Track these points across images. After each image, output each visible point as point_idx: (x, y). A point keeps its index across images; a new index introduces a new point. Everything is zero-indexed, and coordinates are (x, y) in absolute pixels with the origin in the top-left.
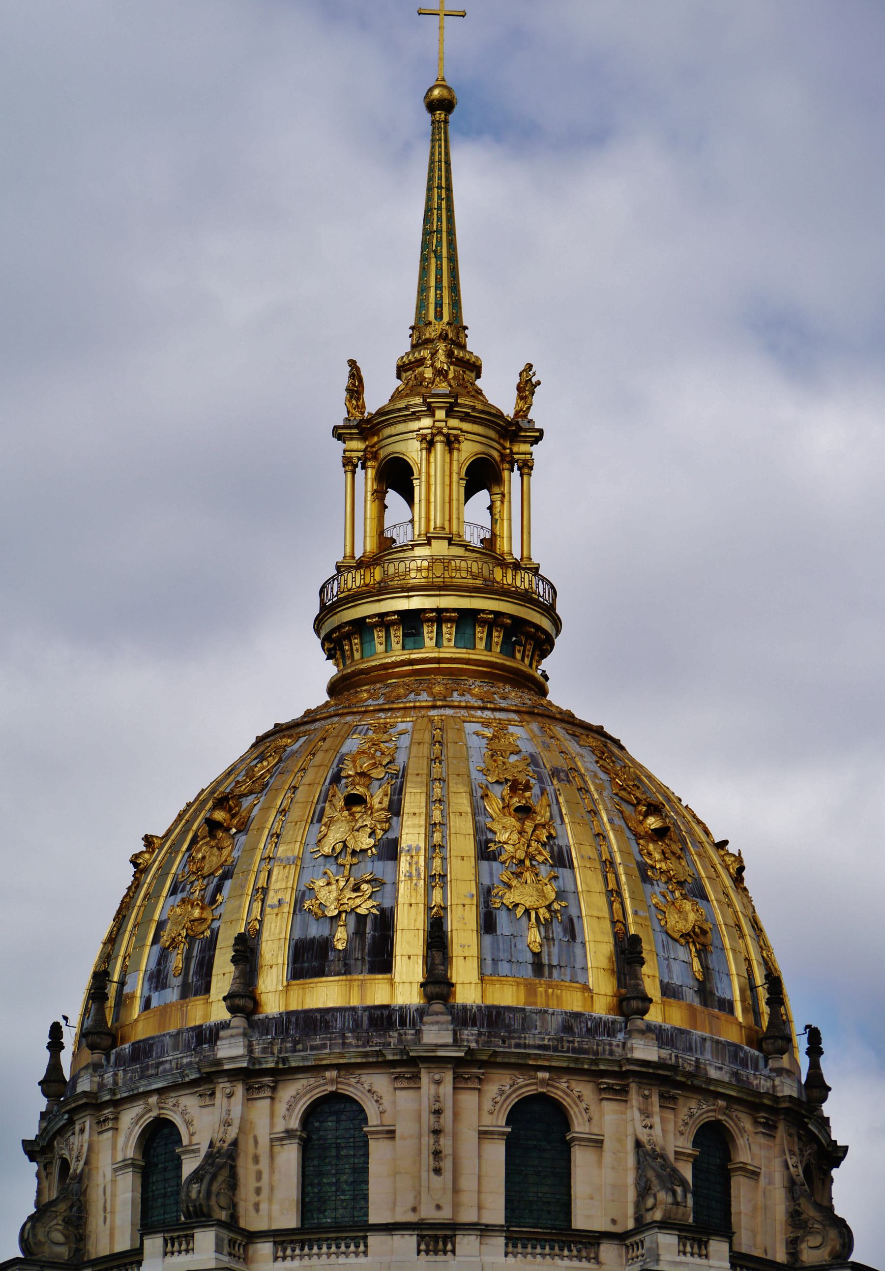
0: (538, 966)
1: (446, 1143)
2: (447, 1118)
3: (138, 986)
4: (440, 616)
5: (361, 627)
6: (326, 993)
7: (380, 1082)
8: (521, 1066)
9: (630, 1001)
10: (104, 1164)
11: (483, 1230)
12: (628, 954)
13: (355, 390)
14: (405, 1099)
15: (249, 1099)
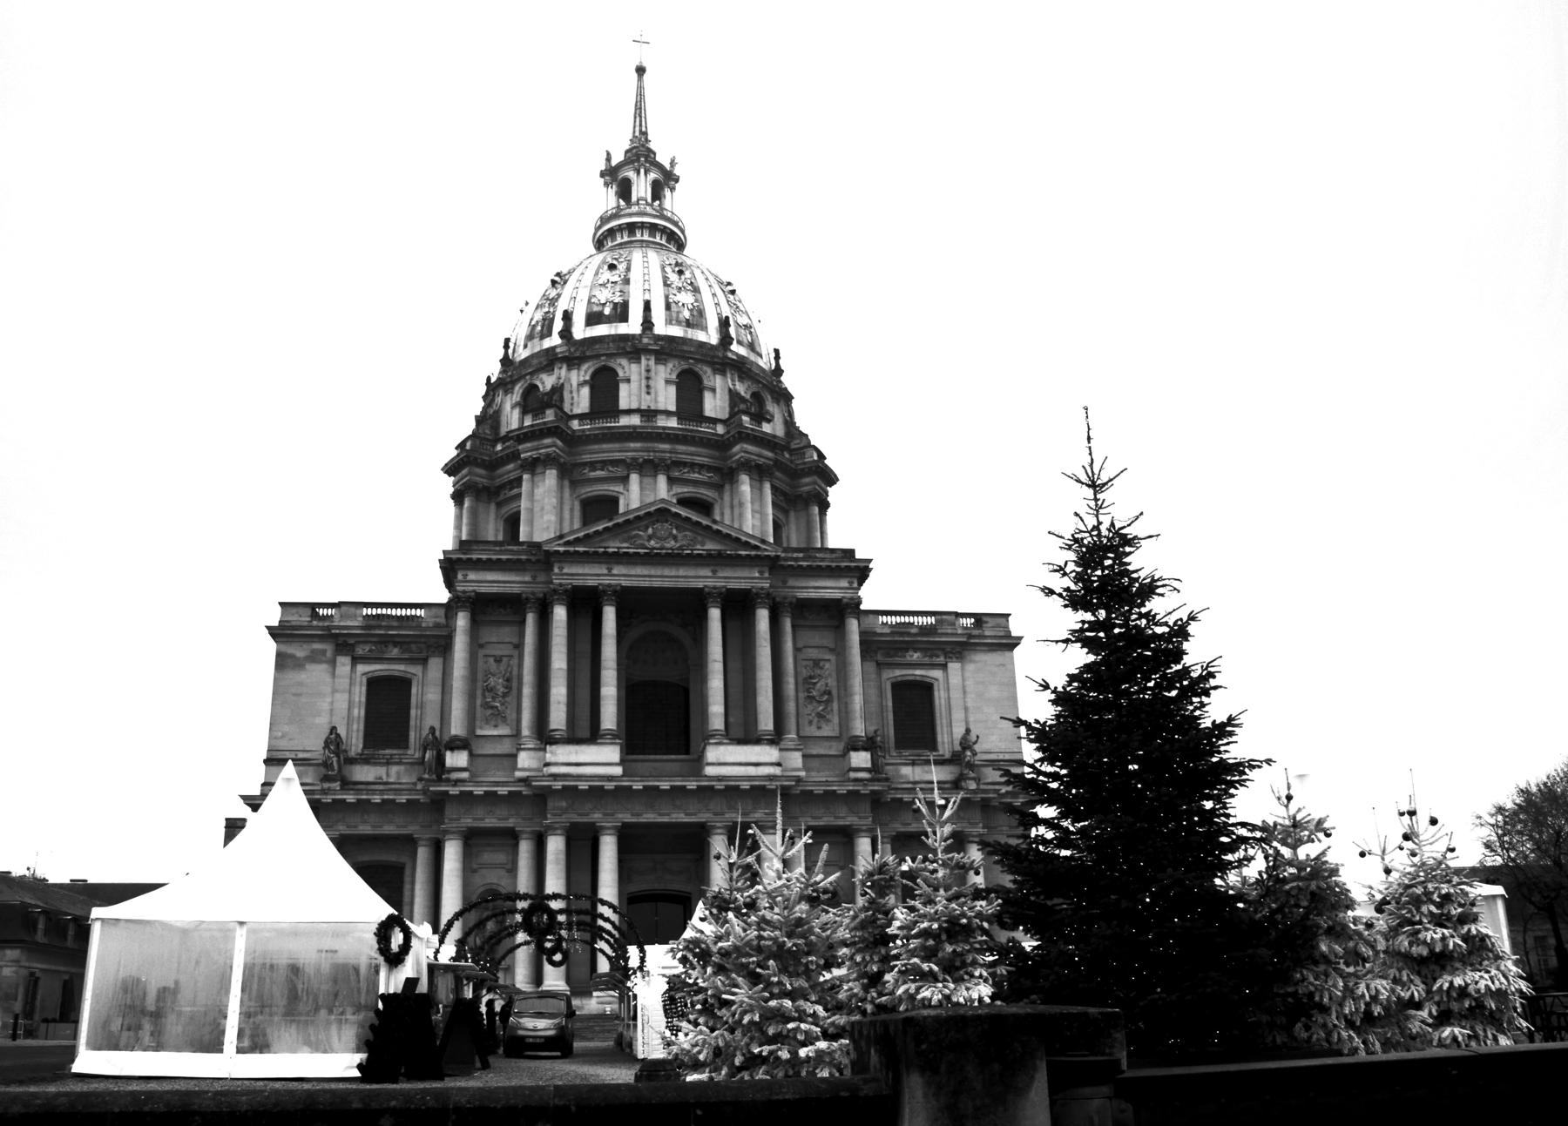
0: (689, 324)
1: (651, 383)
2: (652, 374)
3: (521, 343)
4: (642, 226)
5: (611, 233)
6: (601, 330)
7: (624, 362)
8: (683, 356)
9: (726, 339)
10: (508, 407)
11: (668, 413)
12: (724, 323)
13: (608, 159)
14: (634, 367)
15: (569, 369)
